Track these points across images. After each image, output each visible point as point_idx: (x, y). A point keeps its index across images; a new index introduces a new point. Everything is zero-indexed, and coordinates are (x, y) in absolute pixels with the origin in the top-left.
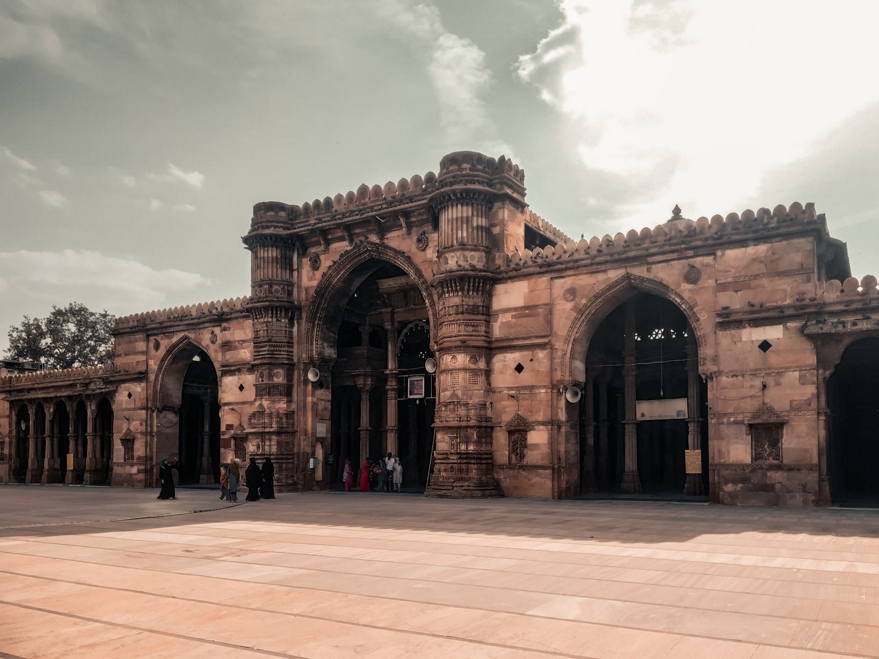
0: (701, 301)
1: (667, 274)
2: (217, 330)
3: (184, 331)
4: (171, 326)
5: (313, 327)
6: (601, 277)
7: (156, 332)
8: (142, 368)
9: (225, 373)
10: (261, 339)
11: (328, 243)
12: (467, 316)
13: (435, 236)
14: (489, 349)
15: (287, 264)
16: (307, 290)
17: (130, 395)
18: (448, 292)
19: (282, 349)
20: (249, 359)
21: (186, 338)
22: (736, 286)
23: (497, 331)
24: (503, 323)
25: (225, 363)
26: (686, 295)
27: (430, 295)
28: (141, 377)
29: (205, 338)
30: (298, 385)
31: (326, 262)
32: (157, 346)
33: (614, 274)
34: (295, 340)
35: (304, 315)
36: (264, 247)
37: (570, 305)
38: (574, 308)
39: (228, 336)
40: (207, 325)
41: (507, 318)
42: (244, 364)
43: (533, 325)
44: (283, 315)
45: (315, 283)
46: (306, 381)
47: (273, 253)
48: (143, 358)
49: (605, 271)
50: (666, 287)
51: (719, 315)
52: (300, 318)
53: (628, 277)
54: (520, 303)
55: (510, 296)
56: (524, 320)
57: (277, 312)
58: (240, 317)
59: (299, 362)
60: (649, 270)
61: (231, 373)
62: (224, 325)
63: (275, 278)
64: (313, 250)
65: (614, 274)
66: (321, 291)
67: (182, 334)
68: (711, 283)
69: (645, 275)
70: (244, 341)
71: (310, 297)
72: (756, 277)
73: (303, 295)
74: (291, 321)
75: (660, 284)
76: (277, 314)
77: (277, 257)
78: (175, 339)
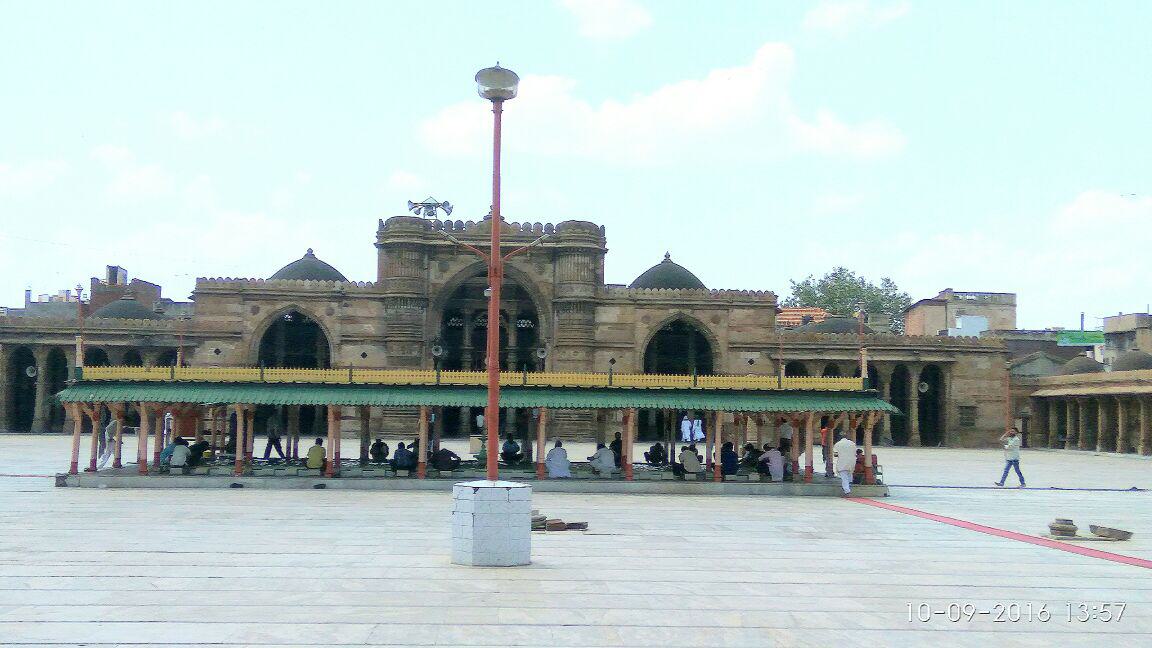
0: (720, 334)
1: (704, 317)
2: (334, 305)
3: (291, 300)
7: (256, 297)
10: (404, 322)
11: (459, 253)
13: (550, 266)
14: (594, 347)
15: (419, 263)
16: (434, 285)
17: (217, 352)
22: (739, 329)
28: (235, 336)
29: (319, 312)
31: (455, 268)
32: (255, 310)
33: (672, 311)
35: (431, 305)
39: (349, 311)
41: (605, 328)
45: (443, 282)
47: (415, 256)
48: (240, 319)
51: (730, 343)
55: (607, 315)
60: (693, 313)
61: (354, 342)
62: (345, 302)
65: (672, 311)
67: (289, 303)
68: (726, 325)
70: (367, 318)
72: (747, 325)
74: (422, 308)
78: (279, 306)
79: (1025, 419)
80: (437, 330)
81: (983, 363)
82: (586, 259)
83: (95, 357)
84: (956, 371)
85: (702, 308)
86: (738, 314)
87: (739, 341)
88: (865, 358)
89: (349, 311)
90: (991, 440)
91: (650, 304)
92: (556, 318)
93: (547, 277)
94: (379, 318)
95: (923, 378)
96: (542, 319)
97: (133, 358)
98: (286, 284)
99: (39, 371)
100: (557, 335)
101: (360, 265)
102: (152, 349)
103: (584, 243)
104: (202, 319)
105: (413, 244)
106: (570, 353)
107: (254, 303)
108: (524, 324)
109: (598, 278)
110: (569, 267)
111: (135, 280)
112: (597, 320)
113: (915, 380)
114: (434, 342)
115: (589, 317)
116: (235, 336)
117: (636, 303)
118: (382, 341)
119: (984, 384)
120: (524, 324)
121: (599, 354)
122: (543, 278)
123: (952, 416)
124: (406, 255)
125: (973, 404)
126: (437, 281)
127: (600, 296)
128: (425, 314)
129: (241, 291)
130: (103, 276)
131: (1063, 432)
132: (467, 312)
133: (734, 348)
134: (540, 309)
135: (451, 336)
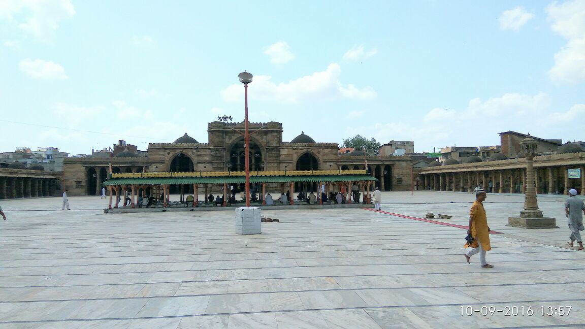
0: (320, 157)
1: (315, 152)
2: (195, 151)
8: (162, 160)
9: (198, 163)
14: (280, 162)
17: (157, 167)
23: (281, 158)
28: (162, 162)
31: (234, 138)
39: (199, 153)
46: (227, 166)
55: (284, 152)
64: (230, 134)
65: (306, 150)
66: (231, 144)
79: (418, 181)
80: (229, 158)
81: (404, 164)
82: (276, 134)
83: (116, 170)
84: (395, 166)
85: (314, 149)
86: (326, 151)
87: (326, 159)
88: (366, 163)
89: (199, 153)
90: (408, 188)
91: (298, 148)
93: (264, 140)
95: (385, 169)
96: (263, 154)
97: (129, 170)
98: (178, 144)
99: (97, 175)
100: (267, 159)
101: (203, 138)
102: (135, 167)
103: (276, 129)
104: (151, 157)
106: (272, 165)
107: (169, 151)
108: (257, 155)
109: (280, 140)
110: (271, 137)
111: (129, 145)
113: (382, 170)
114: (228, 162)
115: (277, 153)
116: (162, 162)
117: (293, 148)
118: (211, 162)
119: (404, 171)
120: (257, 155)
121: (281, 165)
122: (262, 140)
123: (394, 180)
124: (218, 134)
125: (401, 177)
127: (281, 146)
129: (163, 147)
130: (118, 143)
131: (429, 184)
132: (238, 152)
133: (325, 161)
134: (262, 151)
135: (233, 160)
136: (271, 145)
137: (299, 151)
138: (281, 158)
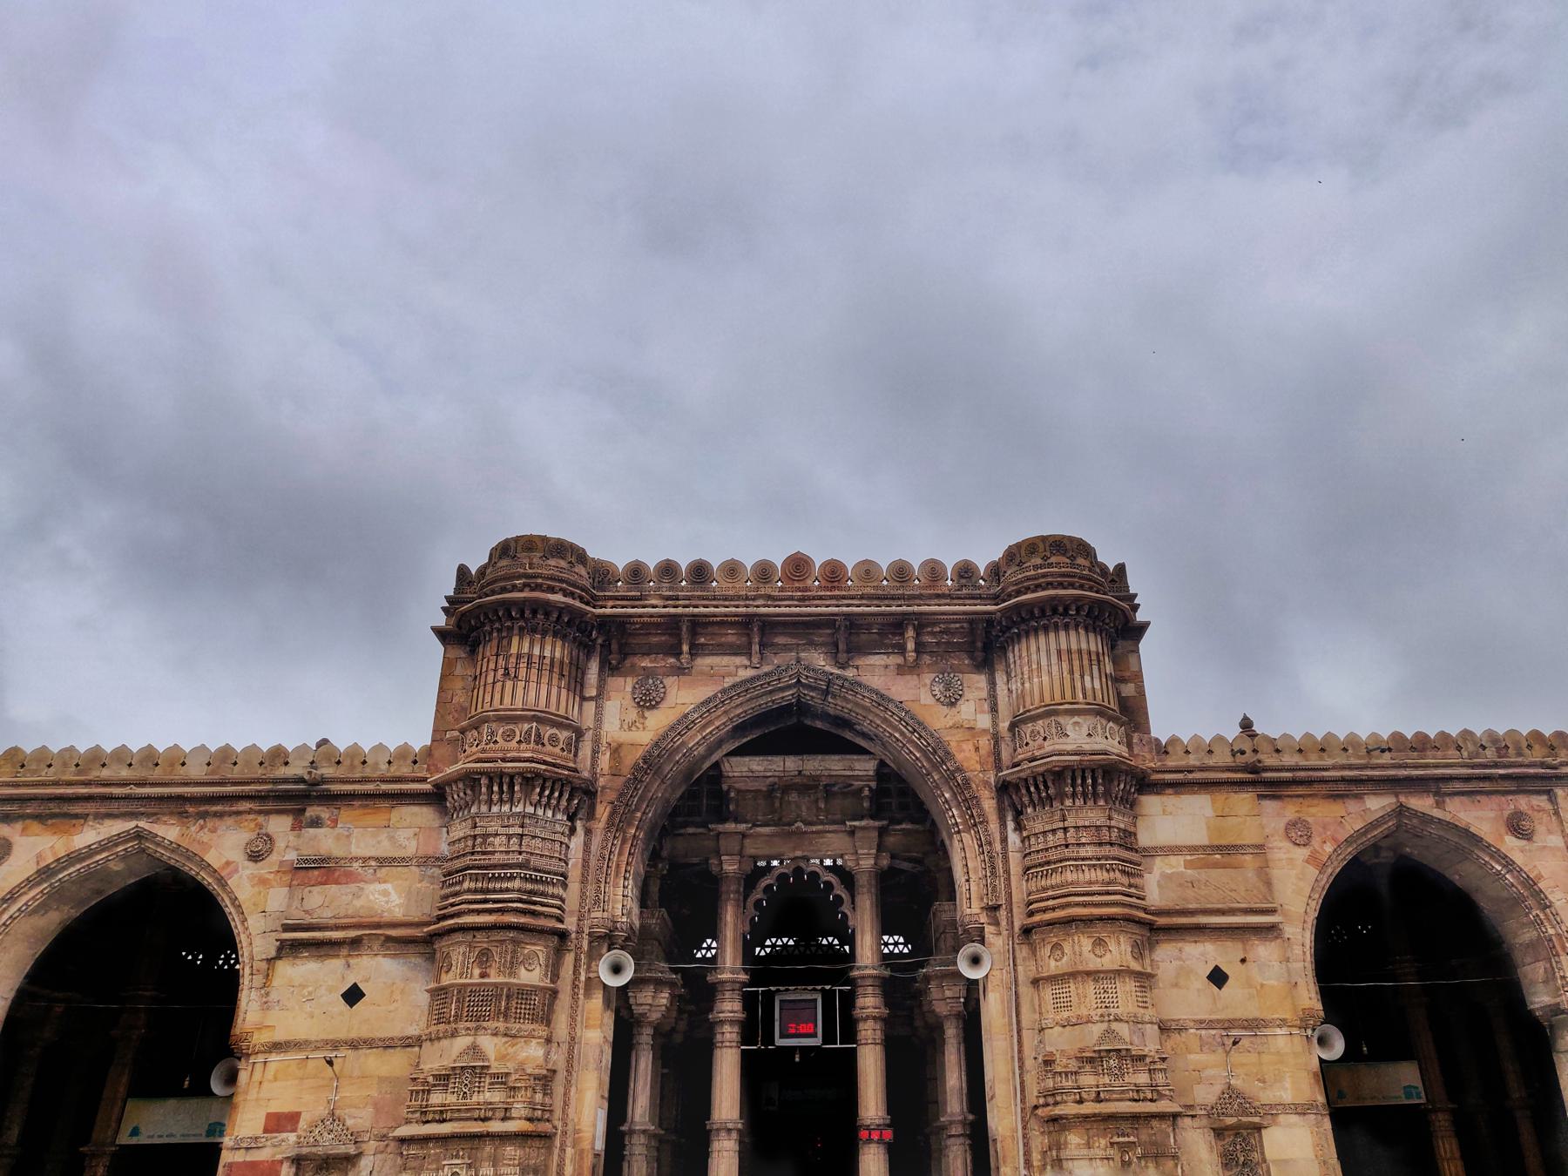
1: (1480, 817)
2: (279, 826)
4: (89, 798)
5: (624, 842)
6: (1352, 806)
9: (289, 949)
12: (1116, 851)
16: (616, 750)
18: (1074, 795)
19: (550, 890)
20: (398, 914)
21: (139, 835)
24: (1164, 876)
25: (297, 916)
26: (1518, 859)
27: (969, 802)
30: (575, 996)
34: (574, 874)
35: (603, 812)
36: (534, 631)
37: (1302, 853)
38: (1312, 859)
39: (324, 841)
40: (245, 806)
41: (1176, 864)
42: (378, 926)
43: (1228, 887)
44: (564, 803)
46: (592, 983)
49: (1359, 797)
50: (1476, 840)
52: (591, 815)
53: (1401, 811)
54: (1200, 837)
56: (1215, 873)
57: (552, 793)
58: (386, 796)
59: (579, 932)
60: (1439, 805)
62: (312, 811)
63: (553, 709)
65: (1377, 804)
69: (1437, 813)
70: (383, 862)
71: (626, 770)
73: (605, 761)
74: (571, 818)
75: (1466, 833)
76: (549, 797)
77: (562, 663)
80: (621, 902)
89: (324, 841)
92: (1013, 838)
94: (425, 861)
105: (547, 608)
112: (1144, 840)
114: (607, 939)
115: (1120, 821)
118: (423, 942)
121: (1168, 957)
126: (626, 737)
128: (577, 842)
136: (1048, 747)
137: (1320, 813)
138: (1158, 886)
